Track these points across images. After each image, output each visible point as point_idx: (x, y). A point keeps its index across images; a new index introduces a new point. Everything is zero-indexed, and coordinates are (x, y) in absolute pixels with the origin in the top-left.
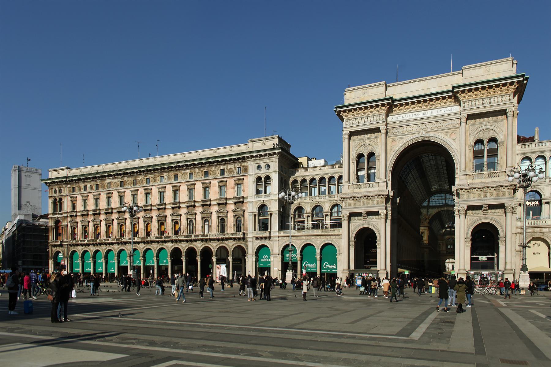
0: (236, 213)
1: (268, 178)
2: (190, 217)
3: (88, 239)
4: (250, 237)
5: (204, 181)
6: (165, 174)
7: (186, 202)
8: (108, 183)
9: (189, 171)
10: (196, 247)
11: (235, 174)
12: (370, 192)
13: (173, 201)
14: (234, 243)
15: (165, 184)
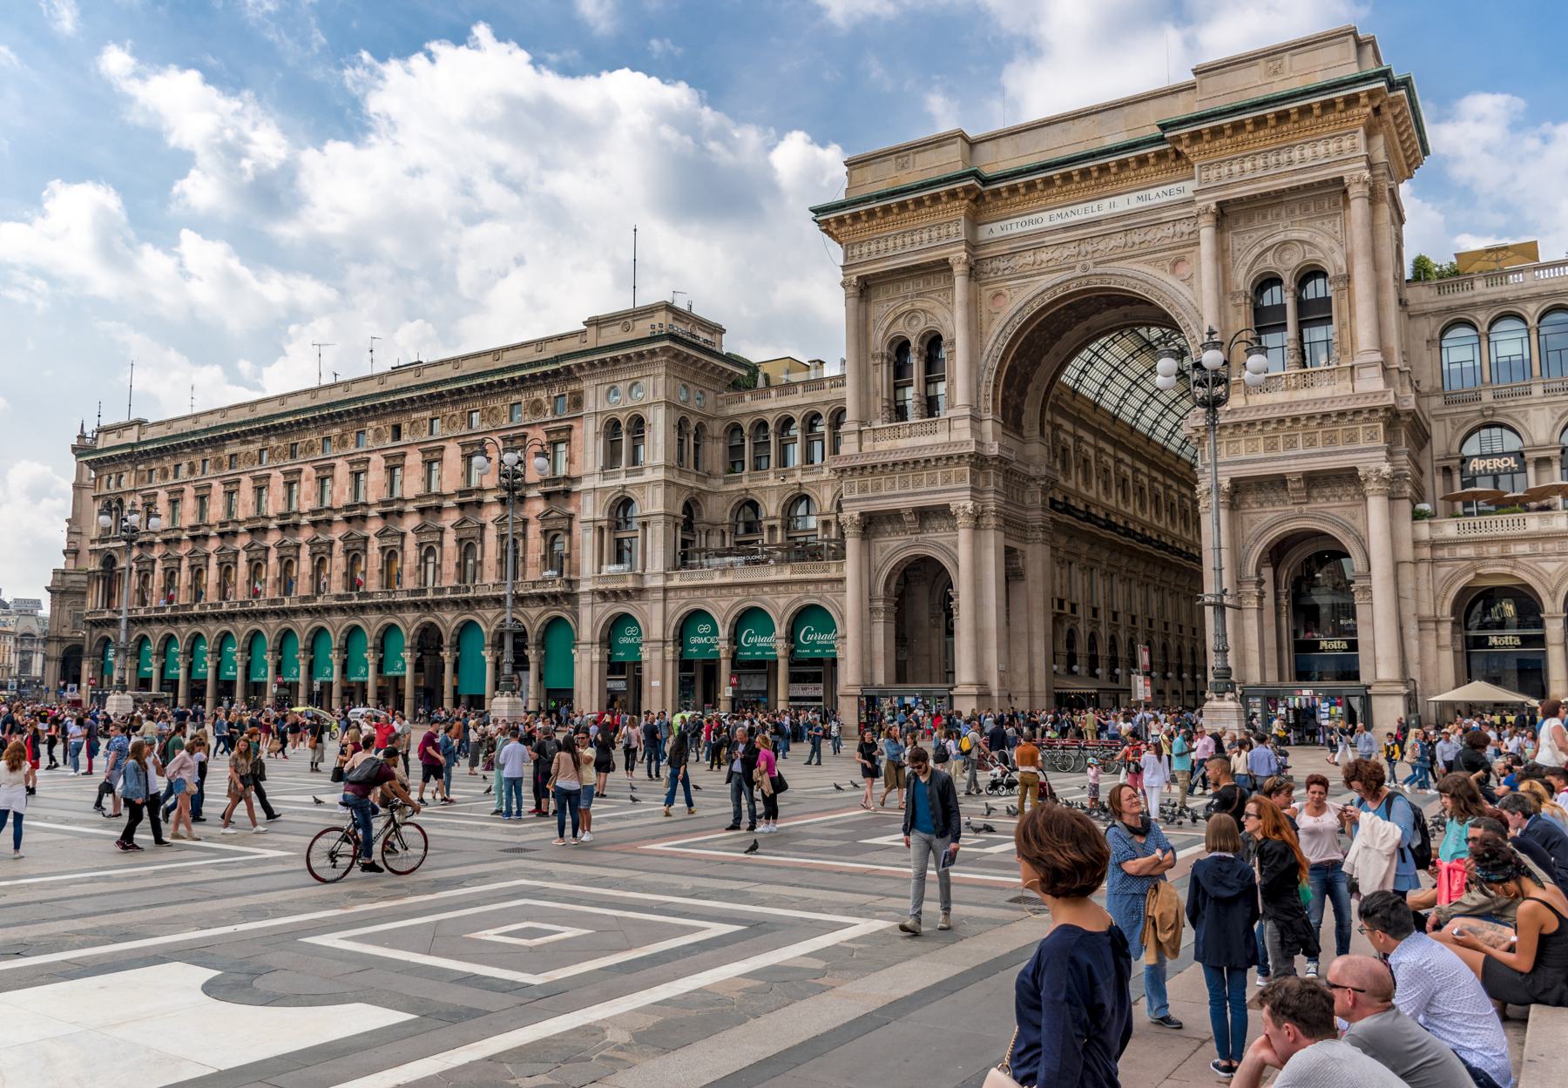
0: (549, 525)
1: (638, 425)
2: (426, 538)
3: (175, 604)
4: (584, 593)
5: (468, 439)
6: (369, 424)
7: (419, 498)
8: (231, 456)
9: (428, 414)
10: (441, 622)
11: (549, 417)
12: (920, 448)
13: (385, 496)
14: (543, 608)
15: (367, 452)
